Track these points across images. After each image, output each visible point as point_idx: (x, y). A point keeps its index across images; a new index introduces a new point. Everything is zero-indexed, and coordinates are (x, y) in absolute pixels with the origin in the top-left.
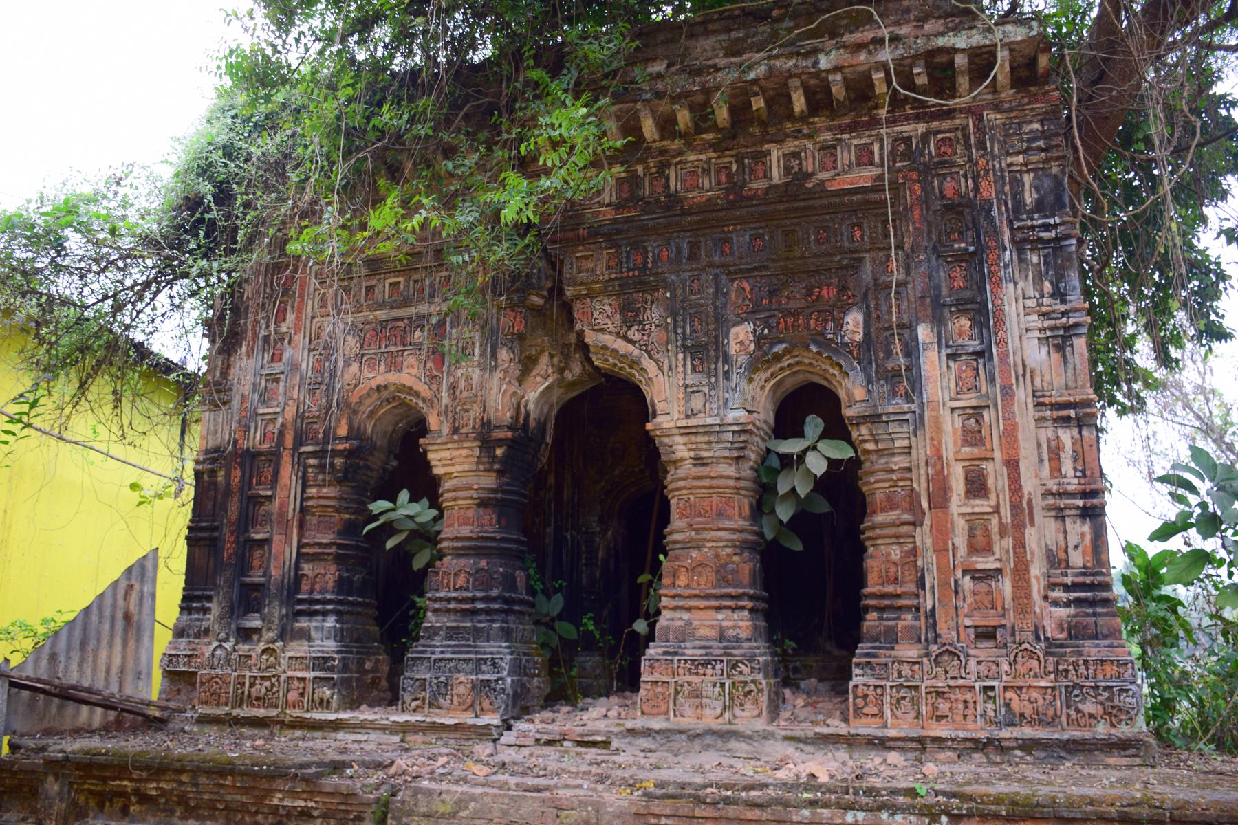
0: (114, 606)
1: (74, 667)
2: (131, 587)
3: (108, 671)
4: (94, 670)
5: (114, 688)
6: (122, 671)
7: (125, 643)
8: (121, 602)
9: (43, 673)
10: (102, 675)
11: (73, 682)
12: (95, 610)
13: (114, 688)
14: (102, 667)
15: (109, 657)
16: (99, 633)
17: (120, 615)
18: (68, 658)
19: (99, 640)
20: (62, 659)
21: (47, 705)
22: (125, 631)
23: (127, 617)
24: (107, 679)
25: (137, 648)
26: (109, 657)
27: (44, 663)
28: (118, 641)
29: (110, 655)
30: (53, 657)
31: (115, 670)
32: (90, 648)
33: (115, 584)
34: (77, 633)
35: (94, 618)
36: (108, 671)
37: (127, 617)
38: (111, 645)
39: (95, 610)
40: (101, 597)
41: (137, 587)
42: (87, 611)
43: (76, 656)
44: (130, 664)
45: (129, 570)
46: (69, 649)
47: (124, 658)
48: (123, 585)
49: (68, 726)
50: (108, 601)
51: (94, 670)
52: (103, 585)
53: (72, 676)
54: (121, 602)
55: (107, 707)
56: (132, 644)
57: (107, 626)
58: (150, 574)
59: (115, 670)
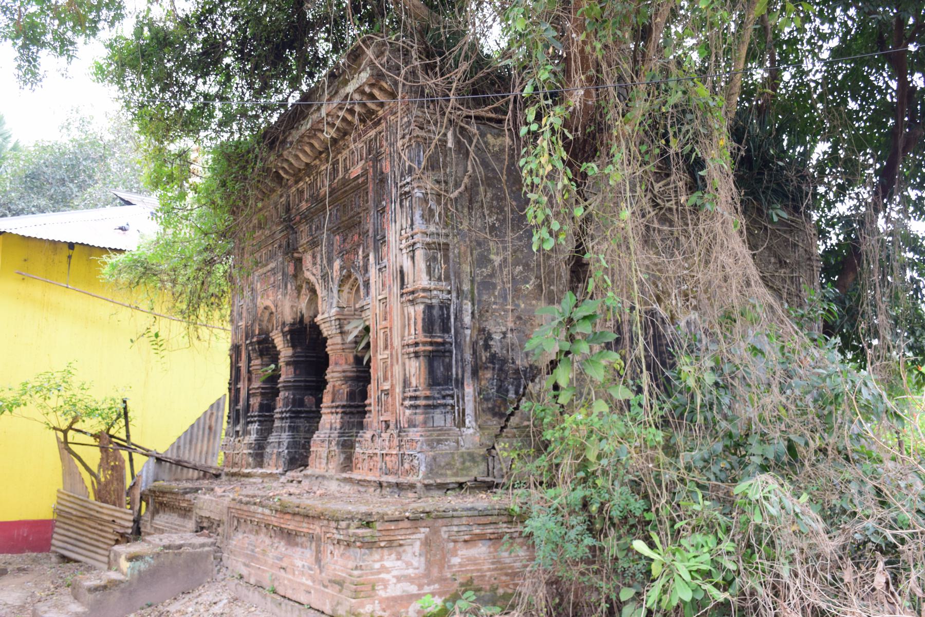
0: (205, 423)
1: (187, 452)
2: (212, 414)
3: (201, 453)
4: (195, 453)
5: (203, 462)
6: (207, 453)
7: (209, 440)
8: (208, 421)
9: (175, 457)
10: (198, 455)
11: (186, 459)
12: (196, 426)
13: (203, 462)
14: (198, 451)
15: (202, 447)
16: (197, 436)
17: (207, 427)
18: (185, 448)
19: (197, 439)
20: (182, 448)
21: (176, 469)
22: (209, 434)
23: (210, 428)
24: (200, 457)
25: (214, 442)
26: (202, 447)
27: (175, 451)
28: (206, 439)
29: (202, 446)
30: (179, 447)
31: (204, 453)
32: (194, 443)
33: (205, 413)
34: (188, 437)
35: (195, 429)
36: (201, 453)
37: (210, 428)
38: (202, 441)
39: (196, 426)
40: (199, 419)
41: (215, 414)
42: (192, 426)
43: (188, 446)
44: (210, 450)
45: (212, 406)
46: (185, 444)
47: (208, 447)
48: (209, 413)
49: (184, 477)
50: (202, 421)
51: (195, 453)
52: (200, 414)
53: (187, 456)
54: (208, 421)
55: (195, 468)
56: (212, 440)
57: (201, 433)
58: (221, 407)
59: (204, 453)
